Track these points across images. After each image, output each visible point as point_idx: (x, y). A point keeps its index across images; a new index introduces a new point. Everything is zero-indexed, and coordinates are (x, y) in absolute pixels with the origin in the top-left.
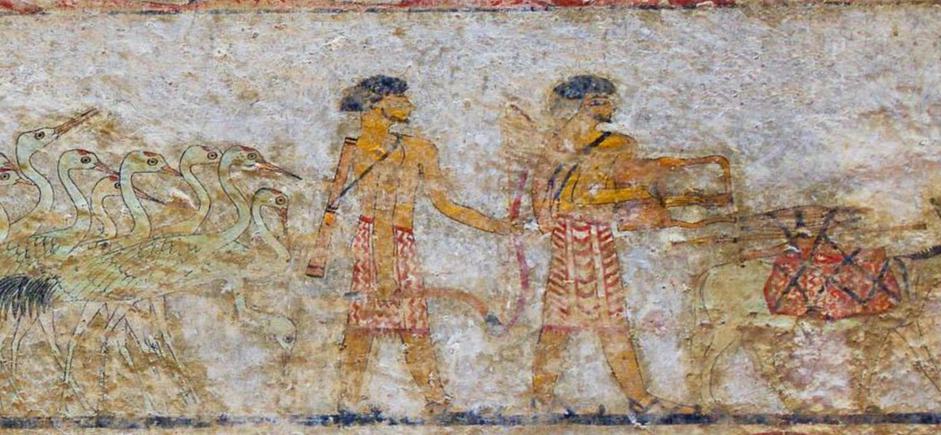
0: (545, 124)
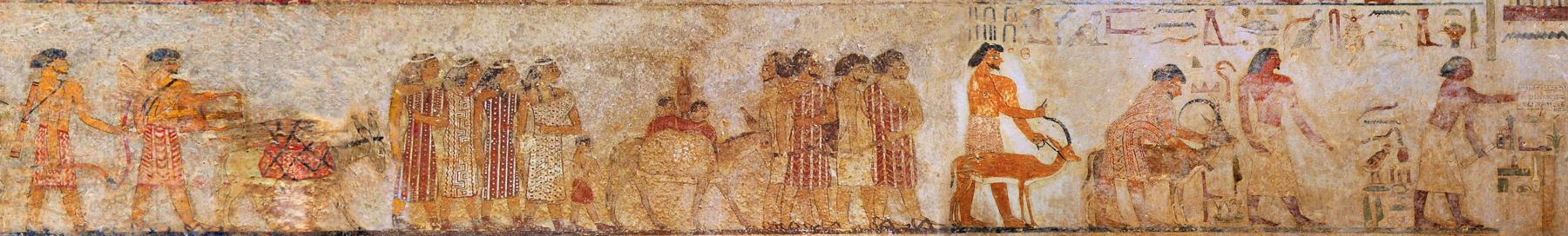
0: (142, 74)
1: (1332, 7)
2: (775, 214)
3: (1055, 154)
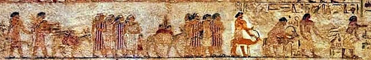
1: (323, 3)
2: (187, 53)
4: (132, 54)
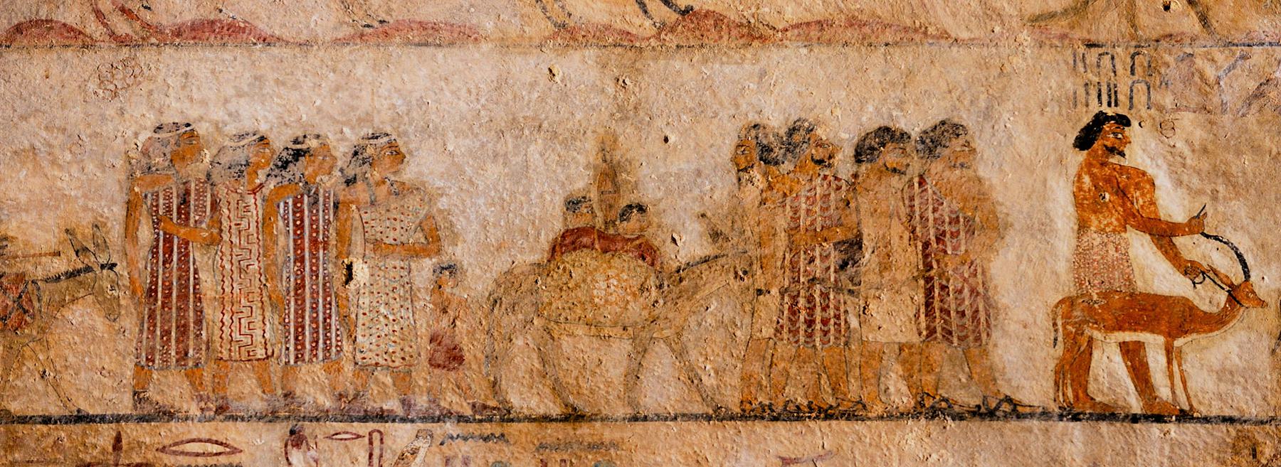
3: (1222, 297)
4: (390, 390)
